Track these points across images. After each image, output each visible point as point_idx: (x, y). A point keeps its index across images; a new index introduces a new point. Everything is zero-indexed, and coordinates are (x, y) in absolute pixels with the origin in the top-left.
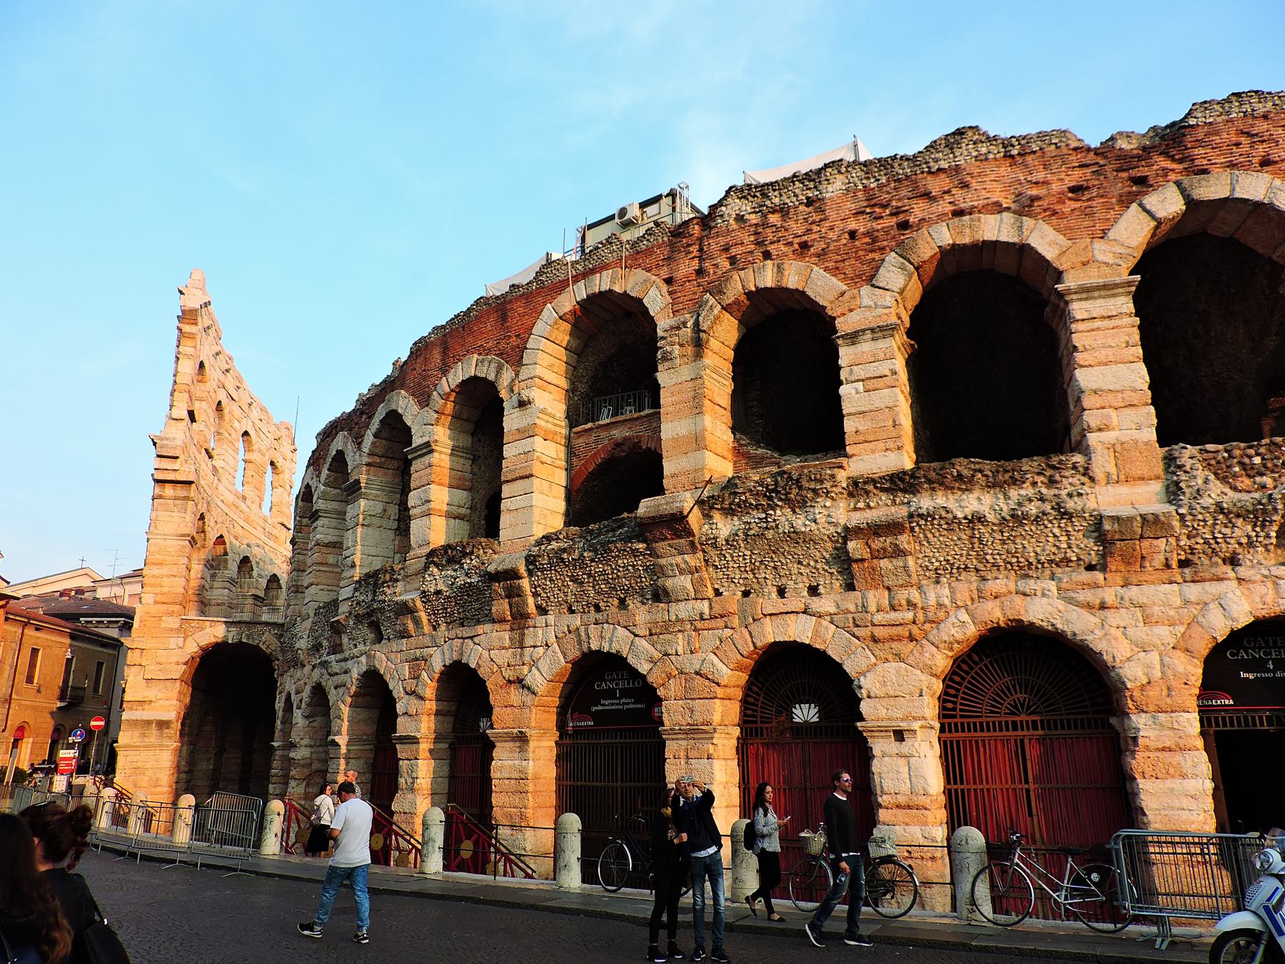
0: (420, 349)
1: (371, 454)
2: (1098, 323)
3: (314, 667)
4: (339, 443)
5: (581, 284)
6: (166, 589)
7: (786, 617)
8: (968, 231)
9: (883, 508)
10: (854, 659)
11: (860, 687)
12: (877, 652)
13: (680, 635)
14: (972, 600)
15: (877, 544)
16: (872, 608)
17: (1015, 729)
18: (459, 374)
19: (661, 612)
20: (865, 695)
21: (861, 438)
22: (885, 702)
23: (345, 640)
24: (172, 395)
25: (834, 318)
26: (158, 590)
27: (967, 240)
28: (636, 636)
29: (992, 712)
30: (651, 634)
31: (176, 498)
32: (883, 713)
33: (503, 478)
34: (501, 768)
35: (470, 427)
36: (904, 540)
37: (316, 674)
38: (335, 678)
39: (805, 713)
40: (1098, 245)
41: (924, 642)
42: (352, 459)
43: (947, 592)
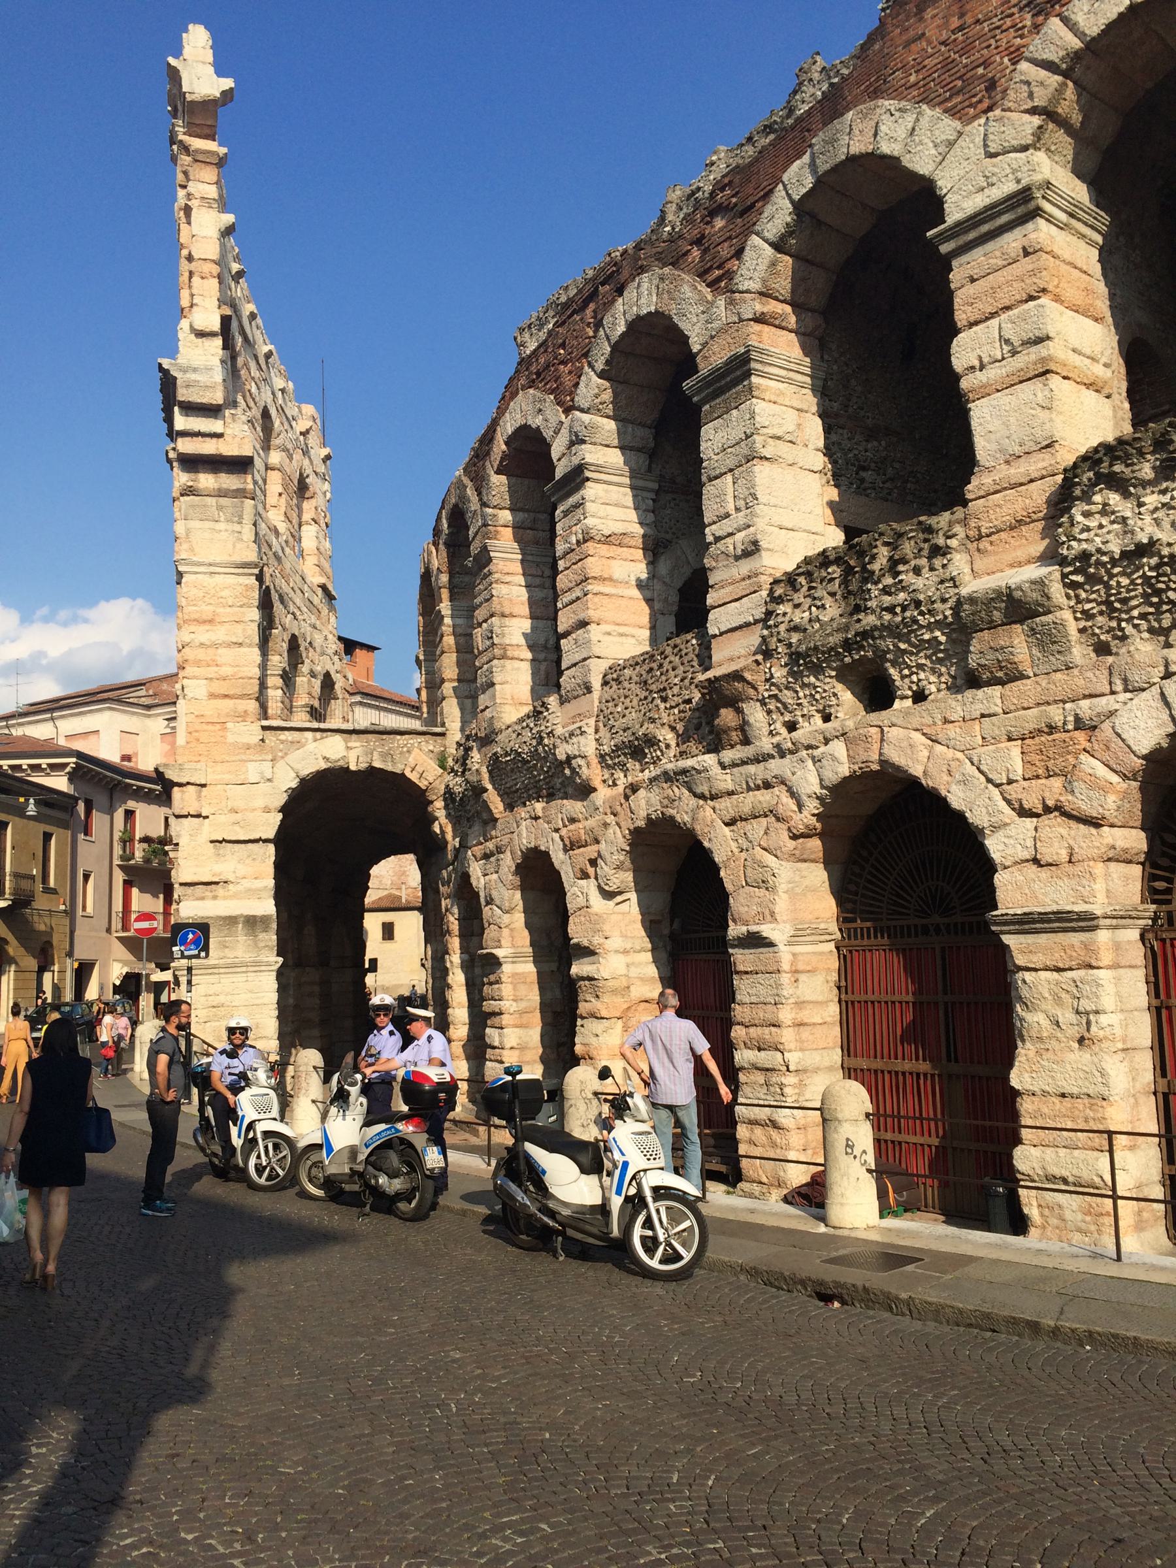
3: (634, 788)
6: (227, 671)
26: (211, 672)
31: (221, 493)
37: (646, 804)
38: (724, 804)
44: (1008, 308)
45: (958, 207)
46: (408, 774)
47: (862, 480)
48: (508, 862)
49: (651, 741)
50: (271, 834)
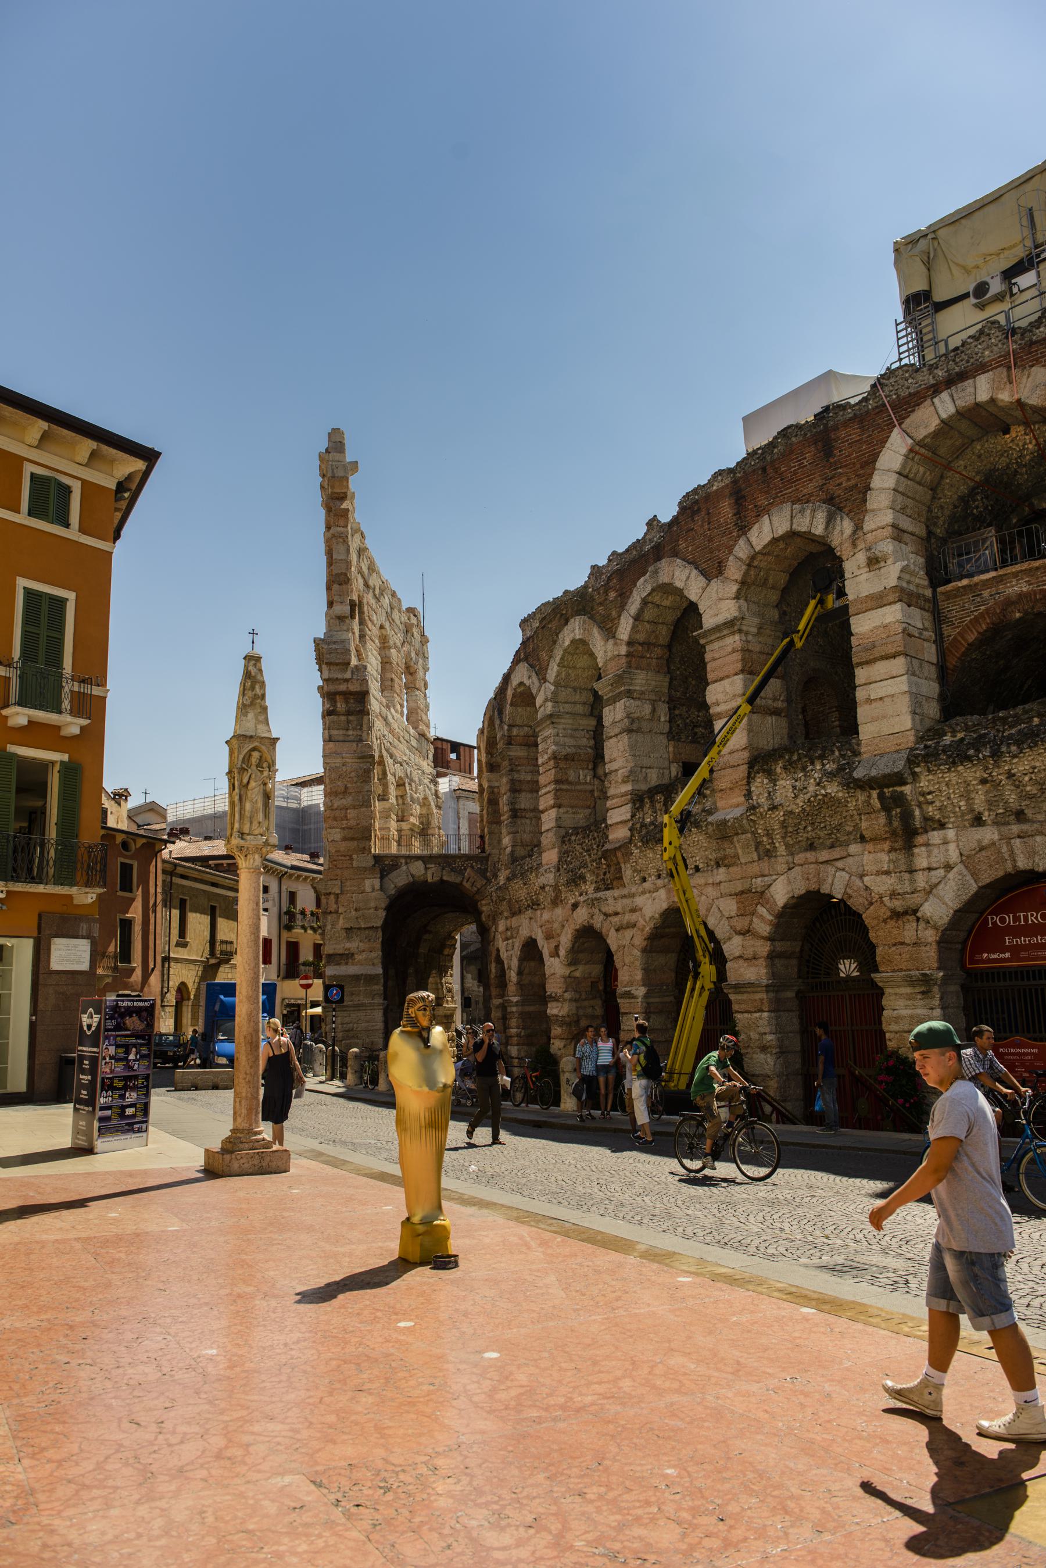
0: (694, 504)
1: (629, 643)
3: (575, 906)
4: (574, 629)
5: (945, 395)
6: (352, 823)
18: (764, 532)
23: (627, 873)
24: (329, 588)
31: (348, 713)
33: (855, 660)
34: (897, 1019)
35: (774, 597)
37: (581, 916)
38: (615, 919)
42: (603, 650)
44: (728, 677)
45: (709, 621)
46: (464, 883)
47: (696, 734)
48: (518, 944)
49: (582, 878)
50: (379, 923)
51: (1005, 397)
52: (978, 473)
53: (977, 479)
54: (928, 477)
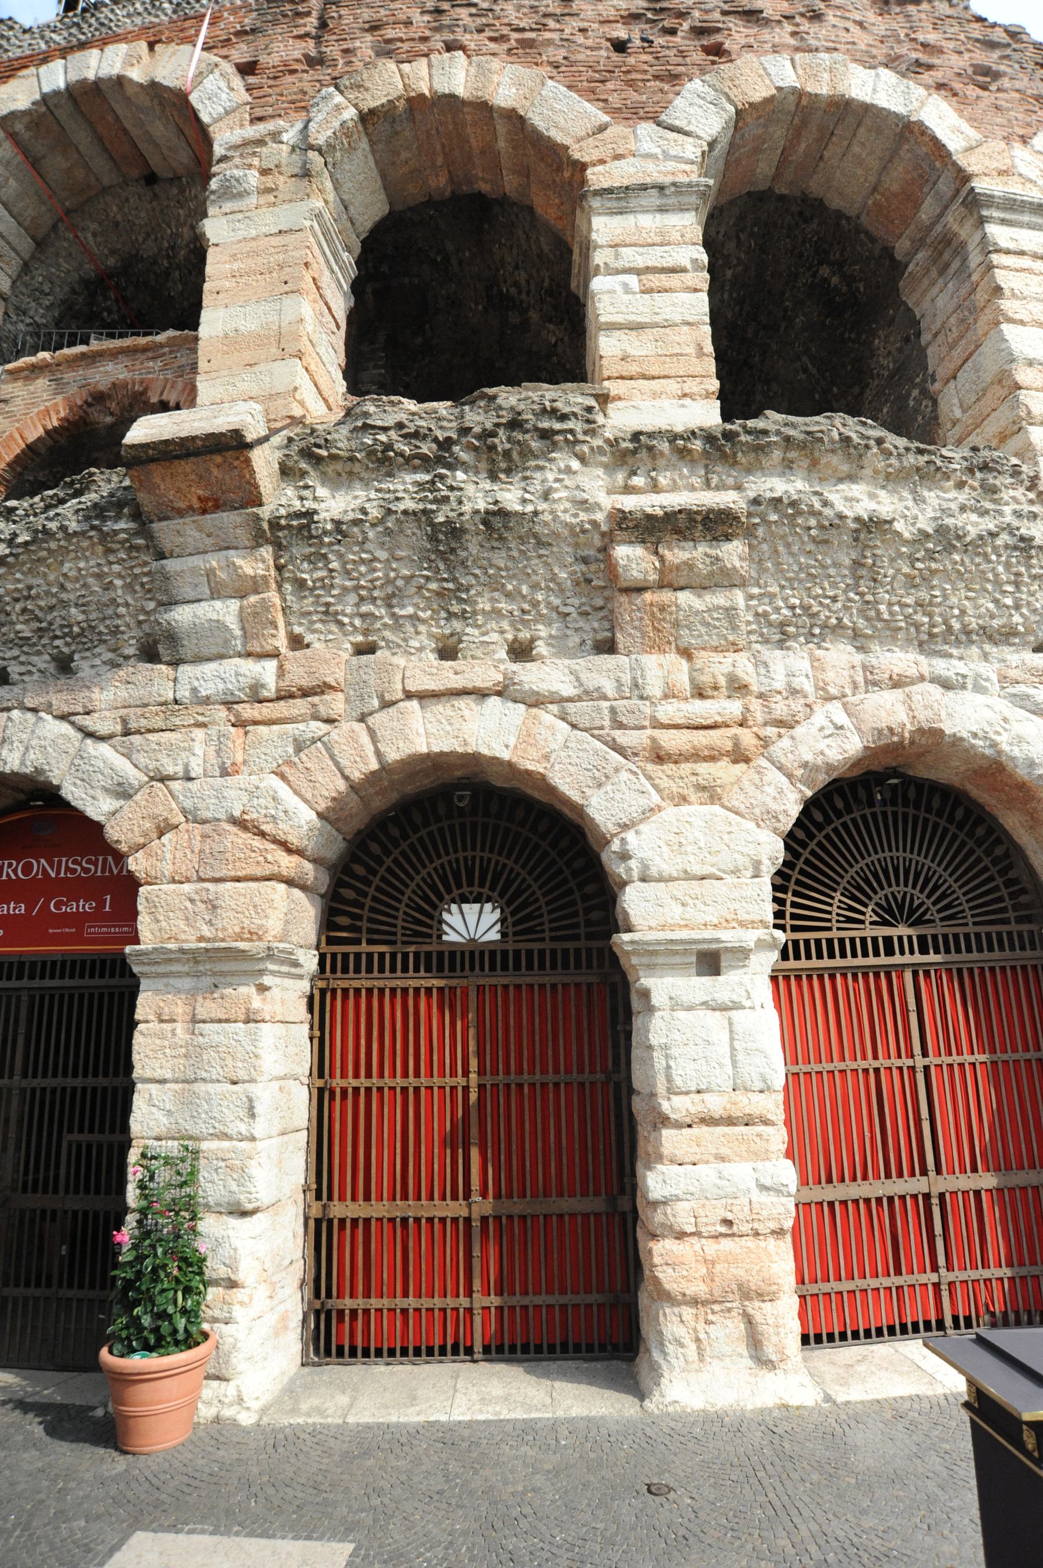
2: (1026, 262)
7: (462, 703)
8: (826, 76)
9: (683, 492)
10: (608, 797)
11: (625, 856)
12: (664, 783)
13: (199, 734)
14: (855, 686)
15: (677, 554)
16: (654, 688)
17: (889, 952)
19: (158, 681)
20: (635, 874)
21: (634, 369)
22: (680, 888)
25: (583, 167)
27: (824, 90)
28: (89, 734)
29: (850, 920)
30: (127, 733)
32: (675, 912)
36: (733, 552)
39: (472, 923)
40: (1020, 154)
41: (763, 762)
43: (805, 665)
51: (136, 75)
52: (113, 252)
53: (111, 262)
54: (31, 212)
